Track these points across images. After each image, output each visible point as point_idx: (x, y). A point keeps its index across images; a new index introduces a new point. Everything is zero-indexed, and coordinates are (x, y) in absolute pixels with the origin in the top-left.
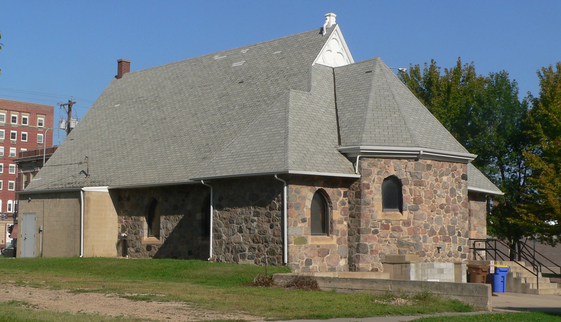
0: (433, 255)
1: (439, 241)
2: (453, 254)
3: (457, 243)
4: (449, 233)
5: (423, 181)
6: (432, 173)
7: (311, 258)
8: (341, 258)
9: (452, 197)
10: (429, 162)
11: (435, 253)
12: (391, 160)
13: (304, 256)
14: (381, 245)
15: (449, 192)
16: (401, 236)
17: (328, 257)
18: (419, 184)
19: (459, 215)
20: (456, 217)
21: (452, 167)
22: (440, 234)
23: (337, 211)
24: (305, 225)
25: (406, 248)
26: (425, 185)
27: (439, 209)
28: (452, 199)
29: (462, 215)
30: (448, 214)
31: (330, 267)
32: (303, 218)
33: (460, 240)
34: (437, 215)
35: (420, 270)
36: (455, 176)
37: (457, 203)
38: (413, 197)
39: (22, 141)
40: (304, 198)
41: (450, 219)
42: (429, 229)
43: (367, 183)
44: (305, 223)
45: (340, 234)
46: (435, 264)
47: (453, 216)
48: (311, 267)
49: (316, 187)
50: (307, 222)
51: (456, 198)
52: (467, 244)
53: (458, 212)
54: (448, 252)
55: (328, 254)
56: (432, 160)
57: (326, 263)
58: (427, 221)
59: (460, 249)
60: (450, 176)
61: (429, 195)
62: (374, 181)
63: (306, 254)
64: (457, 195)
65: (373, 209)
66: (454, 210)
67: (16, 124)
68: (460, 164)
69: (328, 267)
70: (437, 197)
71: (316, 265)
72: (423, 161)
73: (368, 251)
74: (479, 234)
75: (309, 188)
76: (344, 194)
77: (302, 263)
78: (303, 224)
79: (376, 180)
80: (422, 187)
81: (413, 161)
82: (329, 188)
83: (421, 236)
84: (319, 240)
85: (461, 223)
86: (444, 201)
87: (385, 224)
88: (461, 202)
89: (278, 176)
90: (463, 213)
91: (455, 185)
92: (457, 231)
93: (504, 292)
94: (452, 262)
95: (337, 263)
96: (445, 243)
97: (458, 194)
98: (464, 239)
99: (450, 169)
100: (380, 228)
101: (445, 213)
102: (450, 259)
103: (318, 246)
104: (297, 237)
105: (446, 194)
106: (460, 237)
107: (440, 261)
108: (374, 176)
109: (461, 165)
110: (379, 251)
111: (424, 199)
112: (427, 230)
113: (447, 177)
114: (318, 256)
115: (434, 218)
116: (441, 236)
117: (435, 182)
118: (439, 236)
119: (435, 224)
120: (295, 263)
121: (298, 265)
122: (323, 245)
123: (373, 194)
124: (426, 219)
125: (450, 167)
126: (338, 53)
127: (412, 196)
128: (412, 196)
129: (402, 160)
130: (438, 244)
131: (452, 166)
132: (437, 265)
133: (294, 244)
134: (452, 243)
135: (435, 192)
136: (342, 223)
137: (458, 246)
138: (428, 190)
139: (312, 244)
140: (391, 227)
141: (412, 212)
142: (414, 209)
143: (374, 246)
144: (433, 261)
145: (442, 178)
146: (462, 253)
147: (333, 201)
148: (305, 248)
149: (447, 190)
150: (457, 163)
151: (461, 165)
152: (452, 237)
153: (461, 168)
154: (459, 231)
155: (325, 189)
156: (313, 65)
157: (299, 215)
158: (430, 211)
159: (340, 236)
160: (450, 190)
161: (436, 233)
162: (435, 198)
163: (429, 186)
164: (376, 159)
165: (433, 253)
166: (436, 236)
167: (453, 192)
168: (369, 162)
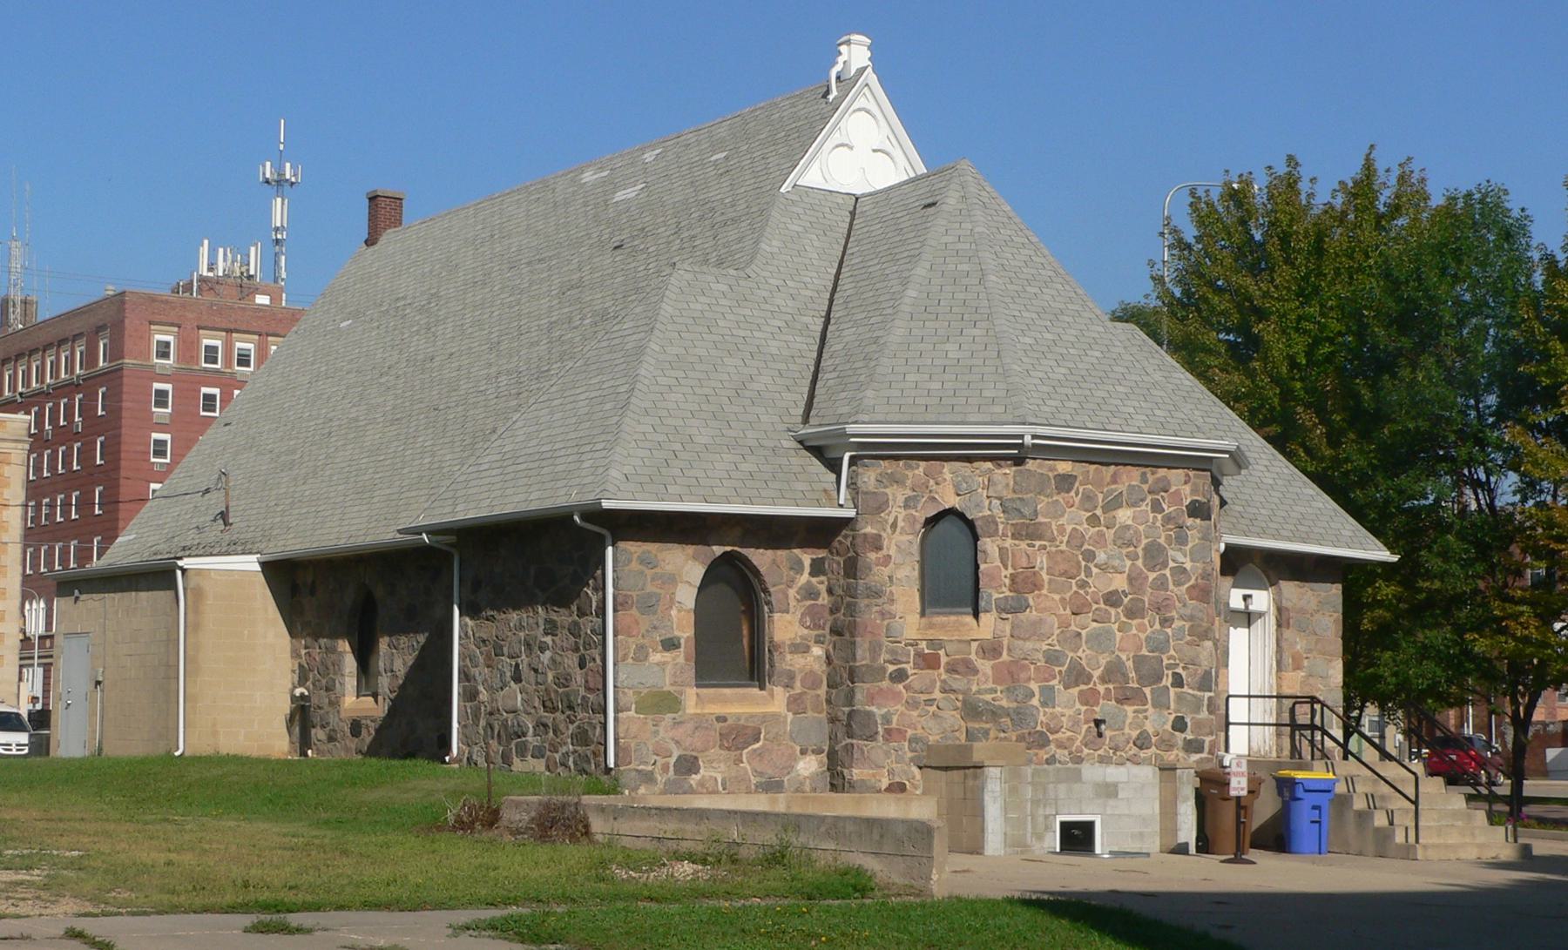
0: (1078, 743)
1: (1101, 701)
2: (1154, 739)
3: (1169, 708)
4: (1140, 679)
5: (1040, 523)
6: (1077, 500)
7: (694, 754)
8: (803, 752)
9: (1152, 569)
10: (1064, 467)
11: (1084, 737)
12: (945, 464)
13: (672, 746)
14: (915, 713)
15: (1141, 553)
16: (974, 688)
17: (755, 750)
18: (1029, 531)
19: (1177, 624)
20: (1169, 631)
21: (1150, 482)
22: (1103, 680)
23: (788, 617)
24: (674, 659)
25: (987, 723)
26: (1048, 534)
27: (1102, 606)
28: (1152, 576)
29: (1187, 625)
30: (1135, 622)
31: (764, 780)
32: (668, 636)
33: (1179, 697)
34: (1095, 624)
36: (1165, 506)
37: (1171, 586)
38: (1011, 570)
39: (203, 413)
40: (672, 580)
41: (1143, 636)
42: (1063, 665)
43: (875, 531)
44: (674, 653)
45: (798, 684)
46: (1083, 771)
47: (1157, 626)
48: (694, 779)
49: (714, 548)
50: (682, 650)
51: (1167, 572)
52: (1205, 708)
53: (1174, 613)
54: (1135, 734)
55: (757, 740)
58: (1055, 642)
59: (1179, 725)
60: (1144, 507)
61: (1063, 567)
62: (894, 525)
63: (677, 742)
64: (1172, 564)
65: (893, 608)
66: (1158, 609)
67: (252, 369)
68: (1180, 471)
69: (754, 780)
70: (1095, 570)
71: (713, 774)
72: (1040, 466)
73: (877, 733)
74: (1311, 681)
75: (690, 549)
76: (811, 565)
77: (665, 768)
78: (668, 656)
79: (900, 524)
80: (1037, 543)
81: (1010, 466)
82: (761, 551)
83: (1034, 686)
84: (726, 701)
85: (1186, 648)
86: (1120, 583)
87: (927, 651)
88: (1186, 586)
89: (582, 518)
90: (1191, 618)
92: (1170, 672)
93: (1320, 853)
94: (1151, 764)
95: (790, 768)
96: (1126, 707)
97: (1173, 561)
98: (1193, 695)
99: (1145, 487)
100: (912, 664)
101: (1124, 619)
102: (1143, 754)
103: (721, 719)
104: (646, 691)
105: (1128, 563)
106: (1180, 690)
107: (1104, 760)
108: (896, 512)
109: (1187, 475)
110: (910, 733)
111: (1045, 577)
112: (1057, 669)
113: (1133, 510)
114: (721, 747)
115: (1084, 633)
116: (1111, 686)
117: (1086, 526)
118: (1101, 688)
119: (1088, 652)
120: (641, 767)
121: (652, 772)
123: (891, 565)
124: (1054, 637)
125: (1144, 480)
126: (874, 151)
127: (1006, 569)
128: (1006, 569)
129: (976, 464)
130: (1097, 709)
131: (1151, 478)
132: (1092, 772)
133: (636, 712)
134: (1149, 706)
135: (1090, 556)
136: (807, 650)
137: (1172, 717)
138: (1062, 552)
139: (699, 711)
140: (944, 660)
141: (1004, 616)
142: (1012, 607)
143: (895, 719)
144: (1079, 760)
145: (1114, 513)
146: (1189, 737)
147: (774, 586)
149: (1132, 549)
150: (1169, 468)
151: (1187, 475)
152: (1152, 692)
153: (1186, 483)
154: (1179, 670)
156: (782, 190)
157: (655, 628)
158: (1068, 612)
159: (798, 688)
160: (1145, 549)
161: (1090, 677)
162: (1089, 573)
163: (1065, 539)
164: (901, 463)
165: (1080, 738)
166: (1090, 686)
167: (1155, 555)
168: (879, 471)
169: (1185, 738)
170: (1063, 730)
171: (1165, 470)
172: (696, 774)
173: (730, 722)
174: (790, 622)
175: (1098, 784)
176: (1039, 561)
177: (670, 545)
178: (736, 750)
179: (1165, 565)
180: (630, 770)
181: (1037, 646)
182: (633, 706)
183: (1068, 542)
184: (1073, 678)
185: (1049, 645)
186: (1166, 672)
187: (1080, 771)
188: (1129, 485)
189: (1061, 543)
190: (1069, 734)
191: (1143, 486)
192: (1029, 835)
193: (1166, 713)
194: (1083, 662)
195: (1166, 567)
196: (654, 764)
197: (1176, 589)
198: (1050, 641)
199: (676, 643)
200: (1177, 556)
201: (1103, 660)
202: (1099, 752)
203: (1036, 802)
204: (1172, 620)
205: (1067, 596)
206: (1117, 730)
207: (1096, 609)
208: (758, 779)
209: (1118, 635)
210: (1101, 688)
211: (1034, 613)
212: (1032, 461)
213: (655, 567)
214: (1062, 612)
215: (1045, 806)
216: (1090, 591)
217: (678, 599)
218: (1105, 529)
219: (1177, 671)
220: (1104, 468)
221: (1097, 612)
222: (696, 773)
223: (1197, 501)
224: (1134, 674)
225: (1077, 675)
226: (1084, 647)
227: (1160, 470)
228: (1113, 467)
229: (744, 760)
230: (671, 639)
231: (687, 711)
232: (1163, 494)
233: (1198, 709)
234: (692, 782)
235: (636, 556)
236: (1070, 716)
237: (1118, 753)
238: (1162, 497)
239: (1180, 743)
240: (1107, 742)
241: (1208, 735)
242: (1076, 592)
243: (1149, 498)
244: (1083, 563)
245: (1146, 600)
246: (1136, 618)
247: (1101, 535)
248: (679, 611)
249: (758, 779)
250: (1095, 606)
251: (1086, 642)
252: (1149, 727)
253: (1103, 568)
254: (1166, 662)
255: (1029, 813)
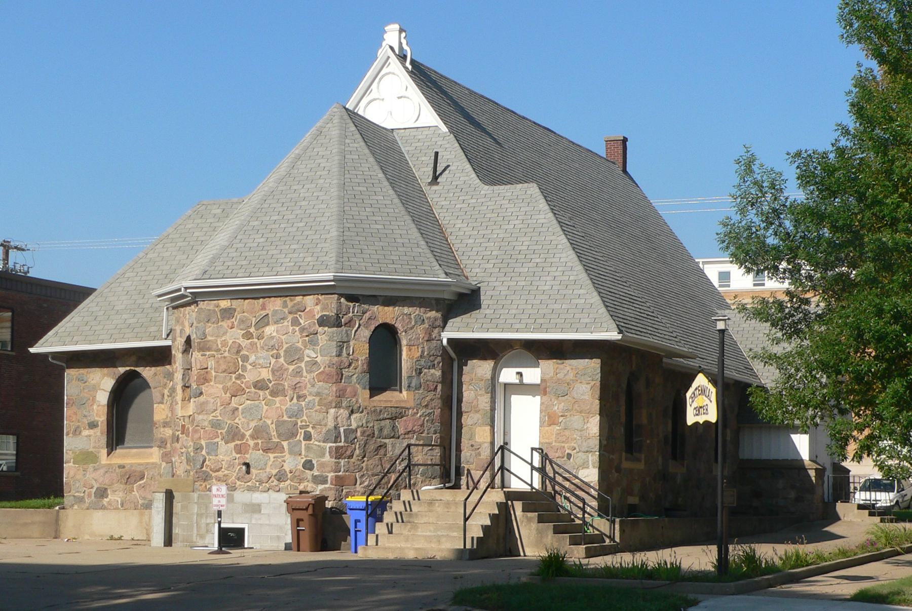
2: (289, 475)
3: (300, 455)
4: (279, 436)
5: (209, 341)
7: (106, 487)
9: (291, 363)
10: (225, 304)
11: (237, 474)
17: (140, 485)
19: (309, 398)
20: (303, 403)
21: (289, 307)
22: (253, 437)
23: (162, 406)
24: (95, 433)
26: (214, 347)
27: (253, 390)
28: (291, 368)
29: (317, 399)
30: (277, 399)
31: (146, 502)
32: (92, 420)
33: (308, 448)
35: (196, 506)
36: (302, 321)
37: (305, 374)
40: (95, 388)
41: (284, 408)
42: (223, 429)
44: (96, 430)
46: (235, 495)
47: (295, 400)
48: (105, 501)
49: (120, 369)
50: (99, 428)
51: (303, 365)
52: (327, 454)
53: (305, 392)
54: (274, 472)
55: (142, 478)
56: (231, 299)
57: (137, 494)
58: (218, 414)
59: (308, 465)
60: (286, 323)
61: (223, 367)
63: (96, 480)
64: (307, 359)
68: (312, 297)
69: (141, 502)
70: (249, 367)
71: (115, 498)
72: (208, 304)
74: (567, 433)
75: (105, 370)
77: (89, 495)
78: (91, 432)
80: (208, 353)
82: (148, 368)
83: (203, 443)
86: (265, 374)
89: (53, 358)
91: (300, 340)
92: (303, 431)
97: (308, 356)
98: (319, 446)
99: (286, 310)
101: (269, 397)
102: (282, 485)
103: (122, 467)
104: (78, 452)
105: (273, 361)
106: (308, 442)
107: (250, 489)
109: (318, 299)
111: (214, 374)
112: (219, 432)
113: (276, 326)
115: (240, 407)
116: (260, 441)
117: (242, 340)
118: (251, 443)
120: (76, 494)
121: (83, 497)
122: (132, 465)
124: (218, 411)
125: (285, 305)
126: (399, 98)
133: (74, 463)
134: (286, 453)
135: (245, 359)
137: (303, 461)
138: (225, 357)
139: (109, 462)
145: (263, 329)
148: (95, 470)
149: (275, 351)
150: (304, 295)
152: (289, 444)
153: (317, 304)
154: (310, 429)
155: (138, 369)
157: (85, 416)
160: (285, 351)
161: (243, 436)
162: (244, 369)
163: (227, 349)
166: (244, 441)
169: (313, 474)
170: (223, 470)
171: (301, 297)
172: (106, 498)
173: (126, 468)
174: (163, 410)
175: (246, 504)
176: (209, 364)
177: (94, 369)
178: (129, 485)
179: (300, 359)
180: (70, 496)
181: (205, 417)
182: (72, 460)
183: (229, 350)
184: (231, 437)
185: (213, 416)
186: (300, 431)
187: (233, 495)
188: (273, 310)
189: (225, 351)
190: (226, 472)
191: (284, 310)
192: (195, 535)
193: (300, 458)
194: (240, 427)
195: (303, 361)
196: (84, 493)
197: (308, 375)
198: (214, 414)
199: (95, 423)
200: (309, 353)
201: (253, 424)
202: (248, 484)
203: (200, 515)
204: (305, 396)
205: (229, 384)
206: (261, 469)
207: (248, 392)
208: (143, 501)
209: (265, 407)
210: (251, 443)
211: (205, 397)
212: (202, 302)
213: (86, 382)
214: (223, 395)
215: (207, 517)
216: (244, 381)
217: (97, 399)
218: (257, 340)
219: (307, 430)
220: (256, 301)
221: (249, 394)
222: (107, 497)
223: (324, 315)
224: (275, 433)
225: (234, 434)
226: (241, 417)
227: (297, 297)
228: (261, 300)
229: (135, 490)
230: (93, 422)
231: (102, 463)
232: (299, 313)
233: (323, 455)
234: (105, 503)
235: (75, 377)
236: (227, 461)
237: (264, 485)
238: (300, 315)
239: (310, 477)
240: (253, 478)
241: (329, 472)
242: (234, 382)
243: (290, 317)
244: (241, 363)
245: (286, 384)
246: (278, 396)
247: (253, 345)
248: (98, 406)
249: (143, 501)
250: (248, 390)
251: (242, 414)
252: (287, 468)
253: (254, 365)
254: (299, 424)
255: (195, 521)
